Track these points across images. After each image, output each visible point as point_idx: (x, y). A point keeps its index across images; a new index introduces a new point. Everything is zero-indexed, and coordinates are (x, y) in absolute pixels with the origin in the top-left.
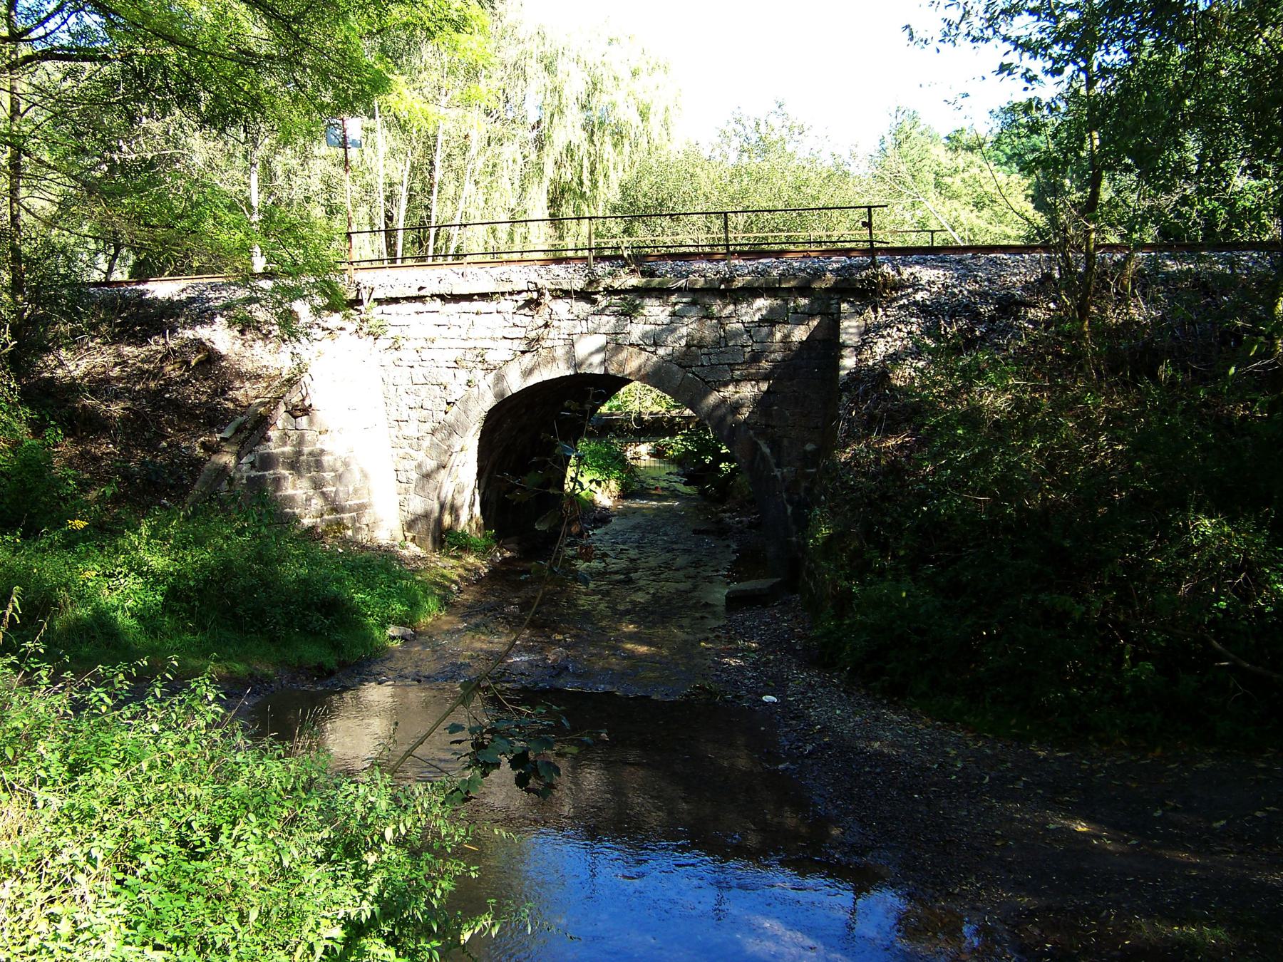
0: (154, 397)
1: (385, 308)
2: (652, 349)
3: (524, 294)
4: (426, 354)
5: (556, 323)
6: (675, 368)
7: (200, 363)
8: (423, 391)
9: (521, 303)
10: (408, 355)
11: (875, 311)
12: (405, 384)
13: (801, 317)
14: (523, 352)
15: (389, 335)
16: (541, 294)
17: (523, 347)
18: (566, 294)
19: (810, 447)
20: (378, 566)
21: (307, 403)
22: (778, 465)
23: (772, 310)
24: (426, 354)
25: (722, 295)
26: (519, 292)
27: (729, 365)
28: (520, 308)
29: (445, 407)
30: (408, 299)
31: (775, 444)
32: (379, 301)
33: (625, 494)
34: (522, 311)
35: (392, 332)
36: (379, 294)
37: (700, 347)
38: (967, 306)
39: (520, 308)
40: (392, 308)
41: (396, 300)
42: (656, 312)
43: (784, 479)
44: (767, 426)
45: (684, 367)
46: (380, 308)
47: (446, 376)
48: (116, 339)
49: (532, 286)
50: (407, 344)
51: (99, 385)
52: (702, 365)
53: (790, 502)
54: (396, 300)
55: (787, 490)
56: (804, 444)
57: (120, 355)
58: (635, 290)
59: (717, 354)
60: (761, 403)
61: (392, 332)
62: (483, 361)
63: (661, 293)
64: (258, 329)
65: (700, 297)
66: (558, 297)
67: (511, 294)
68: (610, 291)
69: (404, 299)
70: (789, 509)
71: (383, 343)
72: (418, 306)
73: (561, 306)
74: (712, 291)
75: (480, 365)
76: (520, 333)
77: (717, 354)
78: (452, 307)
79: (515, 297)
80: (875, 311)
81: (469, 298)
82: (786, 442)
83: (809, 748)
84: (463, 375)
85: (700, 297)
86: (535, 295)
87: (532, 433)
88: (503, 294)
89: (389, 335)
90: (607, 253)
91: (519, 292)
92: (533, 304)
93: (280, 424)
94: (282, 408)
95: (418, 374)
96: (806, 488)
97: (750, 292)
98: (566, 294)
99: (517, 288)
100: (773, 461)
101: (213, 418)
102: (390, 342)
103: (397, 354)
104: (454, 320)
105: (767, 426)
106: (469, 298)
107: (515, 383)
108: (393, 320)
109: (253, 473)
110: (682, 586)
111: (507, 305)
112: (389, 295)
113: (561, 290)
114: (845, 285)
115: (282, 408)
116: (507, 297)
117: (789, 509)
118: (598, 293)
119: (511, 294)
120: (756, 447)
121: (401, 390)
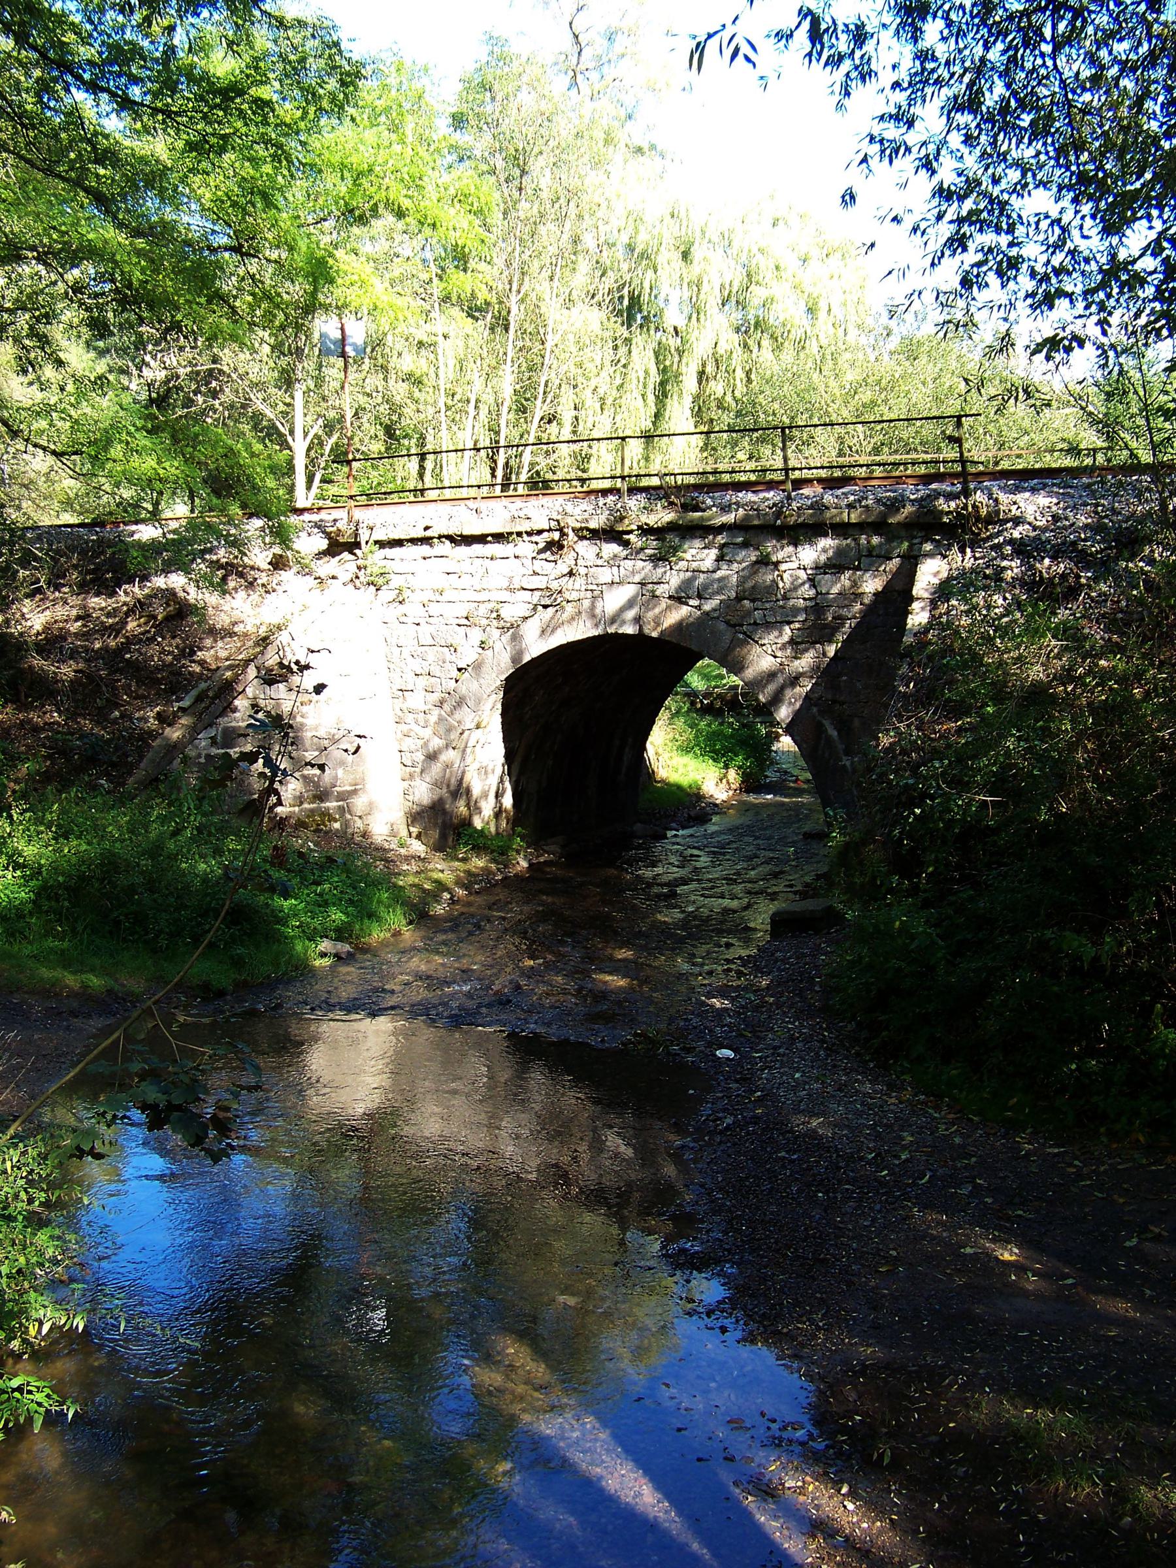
0: (112, 657)
1: (388, 552)
3: (546, 534)
4: (434, 609)
6: (722, 626)
7: (167, 619)
8: (432, 654)
9: (542, 545)
10: (413, 609)
11: (963, 552)
12: (410, 646)
13: (870, 559)
16: (563, 534)
22: (847, 752)
23: (839, 552)
24: (434, 609)
26: (540, 532)
28: (540, 552)
29: (455, 674)
30: (413, 541)
32: (381, 544)
33: (751, 783)
34: (543, 556)
35: (396, 581)
36: (380, 535)
39: (540, 552)
40: (396, 552)
41: (399, 543)
44: (834, 702)
45: (734, 626)
47: (457, 636)
48: (83, 588)
49: (553, 524)
51: (52, 642)
54: (399, 543)
57: (84, 607)
58: (671, 527)
63: (702, 531)
64: (241, 575)
65: (754, 531)
67: (529, 534)
68: (645, 531)
71: (386, 595)
72: (425, 549)
73: (586, 550)
78: (463, 550)
79: (535, 538)
80: (963, 552)
81: (481, 539)
82: (856, 722)
83: (729, 1120)
84: (476, 635)
86: (556, 536)
88: (519, 534)
89: (392, 585)
91: (540, 532)
93: (250, 691)
94: (252, 672)
95: (425, 632)
100: (841, 747)
101: (171, 682)
102: (392, 595)
104: (466, 567)
105: (834, 702)
106: (481, 539)
107: (535, 647)
109: (215, 751)
110: (734, 904)
111: (526, 548)
113: (587, 529)
114: (929, 519)
115: (252, 672)
118: (631, 532)
119: (529, 534)
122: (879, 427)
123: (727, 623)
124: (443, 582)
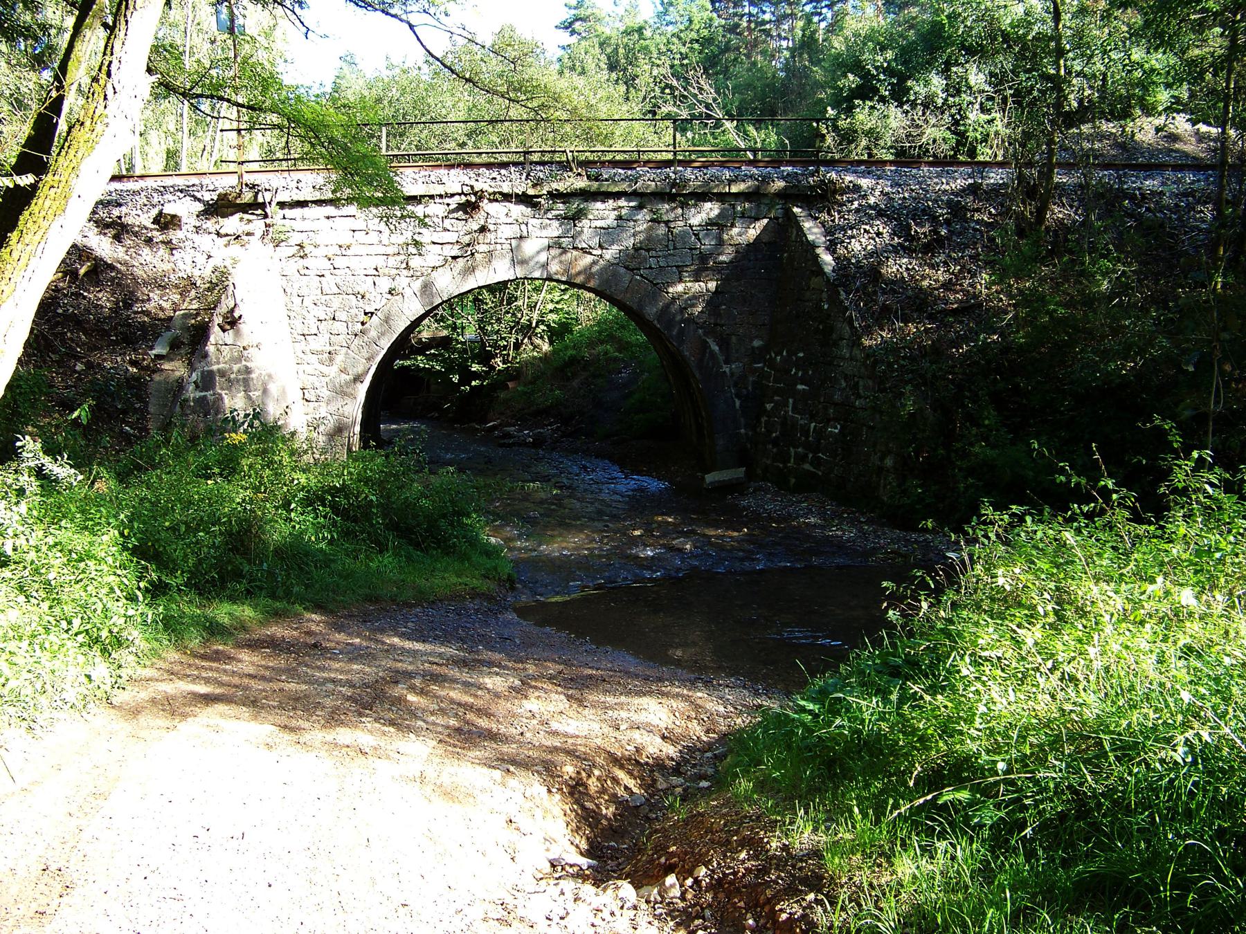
1: (288, 212)
2: (599, 252)
3: (457, 197)
5: (491, 227)
6: (622, 270)
8: (336, 302)
9: (452, 207)
10: (317, 263)
12: (315, 294)
14: (454, 258)
15: (293, 241)
17: (455, 252)
18: (507, 197)
19: (757, 343)
21: (236, 315)
22: (727, 362)
24: (339, 262)
25: (670, 198)
26: (452, 195)
27: (677, 267)
28: (451, 212)
29: (362, 318)
30: (319, 203)
31: (724, 343)
32: (282, 205)
34: (455, 215)
36: (284, 197)
37: (648, 250)
38: (923, 210)
39: (451, 212)
41: (302, 204)
42: (603, 213)
43: (732, 374)
44: (716, 325)
45: (632, 270)
46: (281, 212)
47: (365, 286)
49: (466, 189)
50: (316, 252)
52: (650, 268)
53: (738, 396)
54: (302, 204)
55: (735, 385)
56: (752, 340)
59: (665, 257)
60: (714, 301)
61: (296, 238)
62: (408, 267)
64: (136, 234)
66: (497, 201)
69: (313, 202)
70: (738, 403)
71: (284, 251)
72: (330, 210)
73: (496, 210)
74: (660, 196)
75: (405, 272)
76: (452, 237)
77: (665, 257)
79: (447, 200)
82: (734, 339)
84: (384, 284)
85: (643, 199)
86: (473, 199)
88: (432, 197)
90: (535, 157)
91: (452, 195)
92: (469, 208)
95: (329, 283)
96: (754, 382)
97: (702, 196)
98: (507, 197)
99: (450, 191)
100: (721, 358)
103: (302, 262)
105: (716, 325)
108: (298, 225)
112: (296, 198)
113: (500, 193)
114: (792, 191)
116: (437, 200)
117: (738, 403)
118: (540, 196)
119: (441, 196)
120: (705, 345)
121: (308, 302)
122: (240, 101)
123: (627, 268)
124: (346, 239)
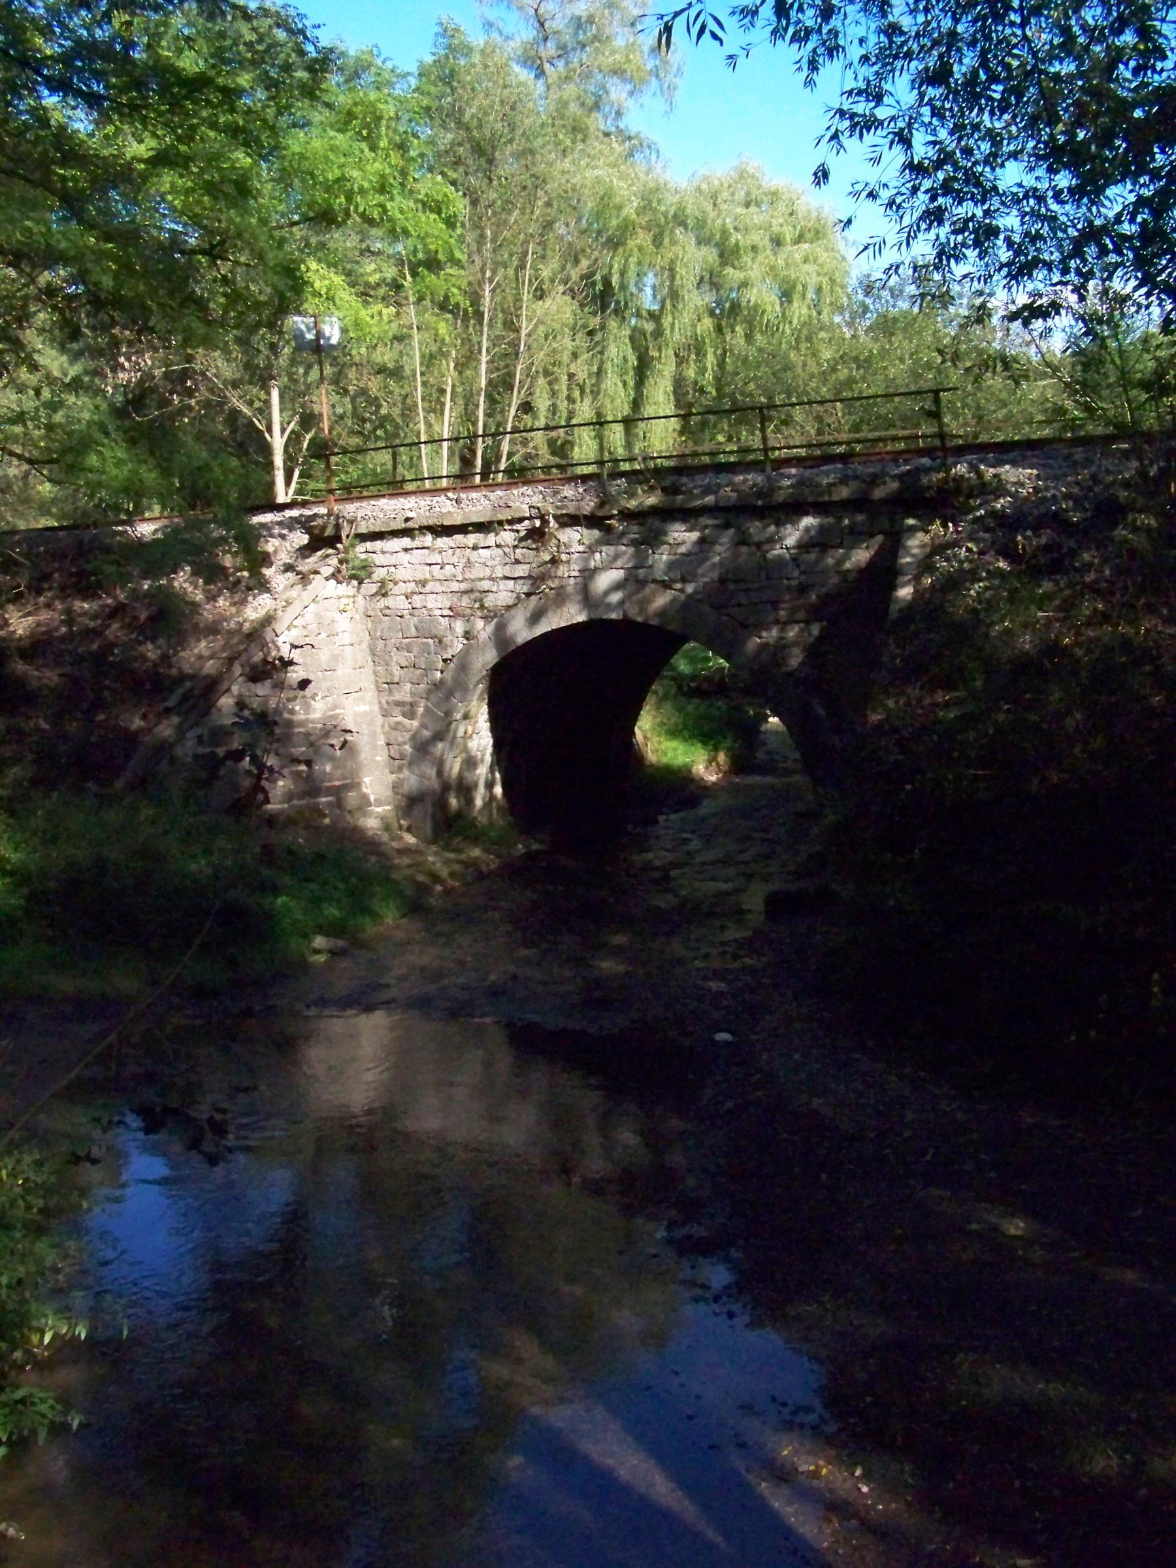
0: (100, 657)
1: (369, 545)
3: (527, 522)
4: (417, 600)
5: (564, 557)
7: (151, 619)
9: (522, 534)
11: (945, 526)
13: (856, 536)
16: (545, 522)
20: (337, 859)
23: (822, 529)
26: (521, 520)
33: (739, 765)
34: (523, 544)
35: (379, 574)
39: (522, 540)
40: (378, 545)
42: (683, 536)
48: (64, 592)
51: (37, 647)
52: (739, 605)
57: (69, 611)
58: (654, 511)
61: (379, 574)
62: (482, 607)
63: (687, 515)
65: (734, 513)
67: (511, 522)
68: (627, 515)
72: (406, 542)
78: (443, 542)
80: (945, 526)
81: (463, 529)
83: (729, 1104)
84: (459, 626)
86: (538, 523)
87: (558, 694)
88: (500, 523)
89: (375, 577)
91: (521, 520)
92: (537, 535)
93: (235, 689)
94: (237, 670)
97: (794, 509)
99: (517, 515)
101: (154, 686)
102: (374, 588)
104: (448, 557)
106: (463, 529)
107: (522, 632)
109: (201, 750)
110: (724, 887)
111: (507, 537)
112: (372, 529)
115: (237, 670)
118: (611, 517)
119: (511, 522)
122: (858, 403)
123: (712, 606)
124: (425, 573)
